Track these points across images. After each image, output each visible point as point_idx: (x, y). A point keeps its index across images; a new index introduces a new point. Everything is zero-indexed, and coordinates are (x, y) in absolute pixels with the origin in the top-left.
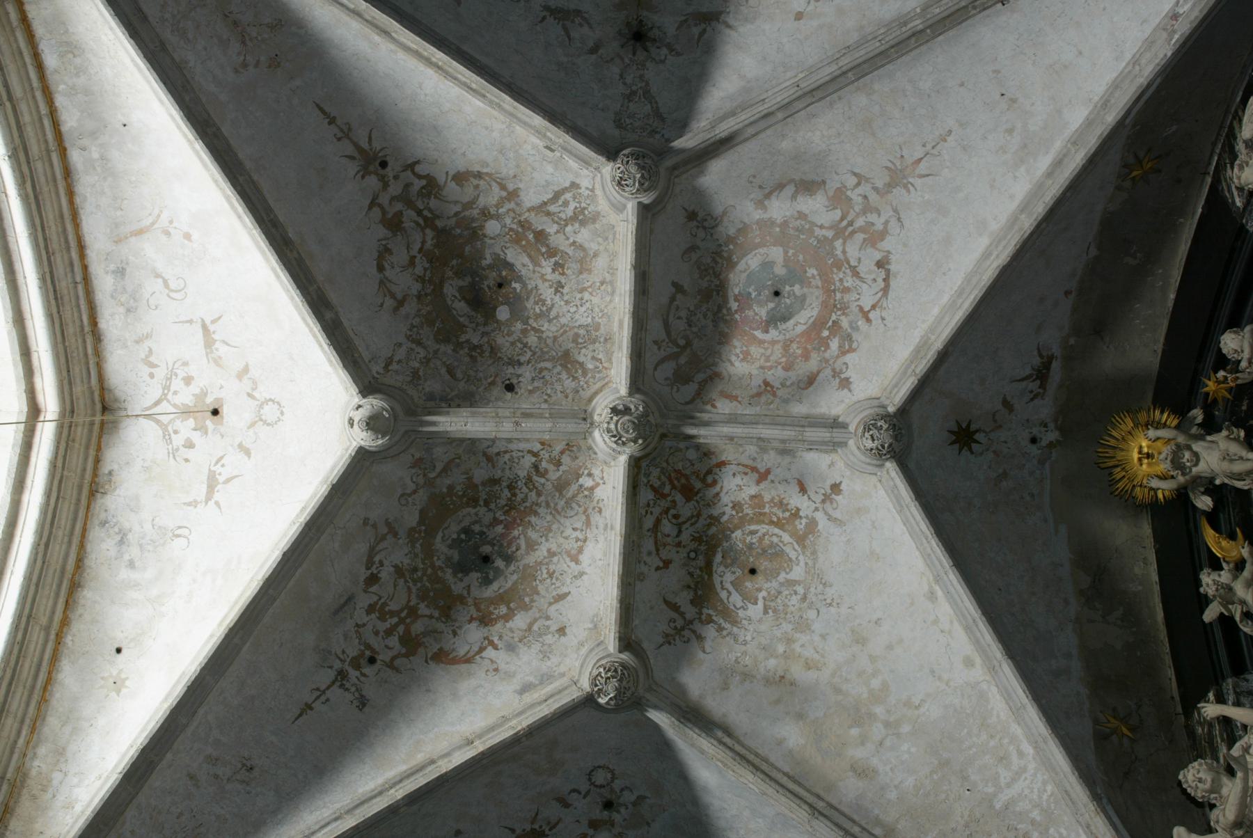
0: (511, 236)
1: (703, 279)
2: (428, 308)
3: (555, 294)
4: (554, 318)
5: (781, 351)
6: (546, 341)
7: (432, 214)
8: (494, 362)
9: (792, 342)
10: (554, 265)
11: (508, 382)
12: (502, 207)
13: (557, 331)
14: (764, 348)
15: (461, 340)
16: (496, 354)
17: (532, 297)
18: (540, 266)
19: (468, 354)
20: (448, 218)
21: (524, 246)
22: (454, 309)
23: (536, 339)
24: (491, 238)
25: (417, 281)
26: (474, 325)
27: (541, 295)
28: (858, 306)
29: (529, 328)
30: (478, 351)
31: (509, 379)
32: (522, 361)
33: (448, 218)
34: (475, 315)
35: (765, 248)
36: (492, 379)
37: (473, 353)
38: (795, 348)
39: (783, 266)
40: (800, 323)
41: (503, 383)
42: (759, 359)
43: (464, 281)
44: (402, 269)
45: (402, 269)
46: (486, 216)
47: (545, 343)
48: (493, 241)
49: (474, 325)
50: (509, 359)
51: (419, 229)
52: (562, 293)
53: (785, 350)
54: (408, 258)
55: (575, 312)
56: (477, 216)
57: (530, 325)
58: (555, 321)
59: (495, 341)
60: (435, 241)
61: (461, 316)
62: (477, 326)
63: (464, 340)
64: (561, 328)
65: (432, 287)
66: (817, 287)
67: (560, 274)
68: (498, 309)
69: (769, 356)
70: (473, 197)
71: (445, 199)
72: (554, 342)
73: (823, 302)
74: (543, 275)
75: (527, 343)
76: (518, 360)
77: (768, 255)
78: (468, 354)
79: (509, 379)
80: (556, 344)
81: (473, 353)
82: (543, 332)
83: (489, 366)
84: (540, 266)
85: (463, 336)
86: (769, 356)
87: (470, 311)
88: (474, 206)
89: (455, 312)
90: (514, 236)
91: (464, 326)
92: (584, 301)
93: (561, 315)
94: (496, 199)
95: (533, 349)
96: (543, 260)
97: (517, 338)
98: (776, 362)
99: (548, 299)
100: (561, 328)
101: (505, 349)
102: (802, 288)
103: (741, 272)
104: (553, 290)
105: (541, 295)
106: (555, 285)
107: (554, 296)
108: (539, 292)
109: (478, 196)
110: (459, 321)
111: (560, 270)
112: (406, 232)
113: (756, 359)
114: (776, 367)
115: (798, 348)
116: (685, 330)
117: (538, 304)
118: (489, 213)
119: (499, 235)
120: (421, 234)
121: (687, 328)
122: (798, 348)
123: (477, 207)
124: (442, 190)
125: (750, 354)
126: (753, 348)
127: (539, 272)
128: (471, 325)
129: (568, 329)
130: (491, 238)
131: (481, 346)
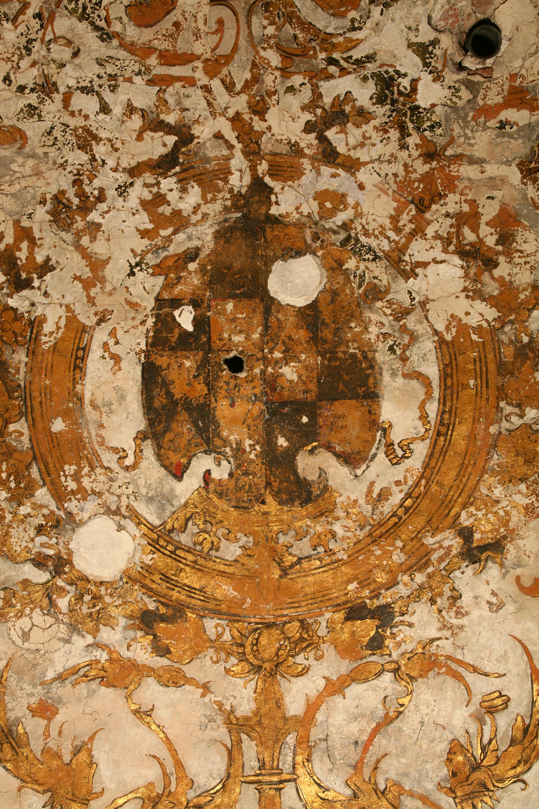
0: (77, 477)
2: (498, 492)
3: (101, 198)
4: (169, 129)
6: (247, 86)
7: (240, 741)
8: (458, 158)
10: (27, 284)
11: (471, 63)
12: (26, 583)
13: (191, 82)
15: (491, 313)
16: (427, 178)
17: (173, 249)
18: (72, 319)
19: (508, 254)
20: (206, 688)
21: (67, 414)
22: (424, 417)
23: (272, 116)
24: (138, 520)
25: (456, 598)
26: (411, 322)
27: (144, 234)
29: (263, 167)
30: (469, 236)
31: (460, 68)
32: (371, 88)
33: (206, 688)
34: (382, 347)
36: (508, 114)
37: (491, 241)
41: (487, 73)
43: (322, 471)
44: (470, 677)
45: (470, 677)
46: (97, 598)
47: (256, 79)
48: (141, 508)
49: (411, 322)
50: (404, 133)
51: (315, 734)
52: (77, 182)
54: (420, 685)
55: (87, 90)
56: (122, 622)
57: (253, 168)
58: (171, 119)
59: (394, 219)
60: (300, 659)
61: (426, 382)
62: (407, 312)
63: (480, 306)
64: (170, 80)
65: (429, 541)
67: (33, 242)
68: (301, 302)
70: (83, 688)
71: (164, 753)
72: (228, 59)
74: (87, 285)
75: (309, 128)
76: (380, 99)
78: (508, 254)
79: (460, 68)
80: (225, 49)
81: (491, 241)
82: (236, 119)
83: (481, 162)
84: (72, 319)
85: (473, 321)
87: (386, 377)
88: (103, 656)
89: (432, 408)
90: (70, 469)
91: (441, 343)
92: (33, 99)
93: (136, 122)
94: (24, 623)
95: (306, 94)
96: (48, 327)
97: (326, 170)
99: (133, 201)
100: (170, 80)
101: (386, 169)
104: (94, 216)
105: (144, 234)
106: (80, 224)
107: (111, 193)
108: (142, 244)
109: (60, 678)
110: (445, 376)
111: (22, 255)
112: (357, 767)
117: (177, 213)
118: (80, 598)
119: (109, 512)
120: (320, 717)
123: (97, 645)
124: (150, 785)
127: (91, 301)
128: (421, 329)
129: (153, 61)
130: (138, 520)
131: (447, 241)
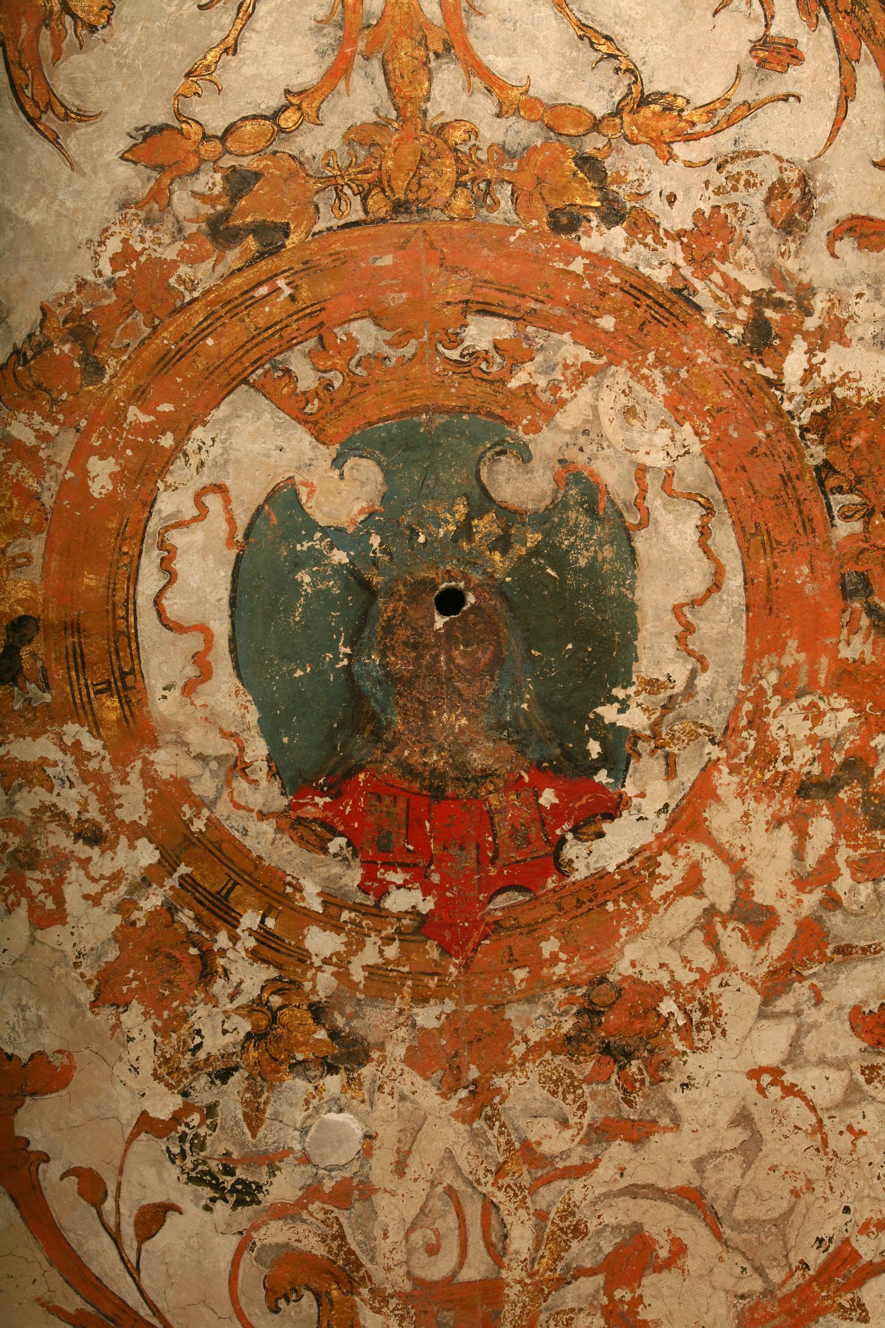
1: (59, 916)
5: (762, 812)
9: (757, 721)
14: (681, 891)
28: (833, 237)
35: (179, 472)
38: (800, 727)
39: (338, 462)
40: (696, 603)
42: (722, 964)
53: (767, 790)
66: (585, 372)
69: (743, 896)
73: (671, 404)
77: (220, 489)
86: (743, 896)
98: (802, 883)
102: (524, 455)
103: (189, 688)
113: (704, 978)
114: (832, 902)
115: (815, 716)
116: (245, 1244)
121: (245, 1212)
122: (815, 716)
125: (657, 992)
126: (632, 951)
